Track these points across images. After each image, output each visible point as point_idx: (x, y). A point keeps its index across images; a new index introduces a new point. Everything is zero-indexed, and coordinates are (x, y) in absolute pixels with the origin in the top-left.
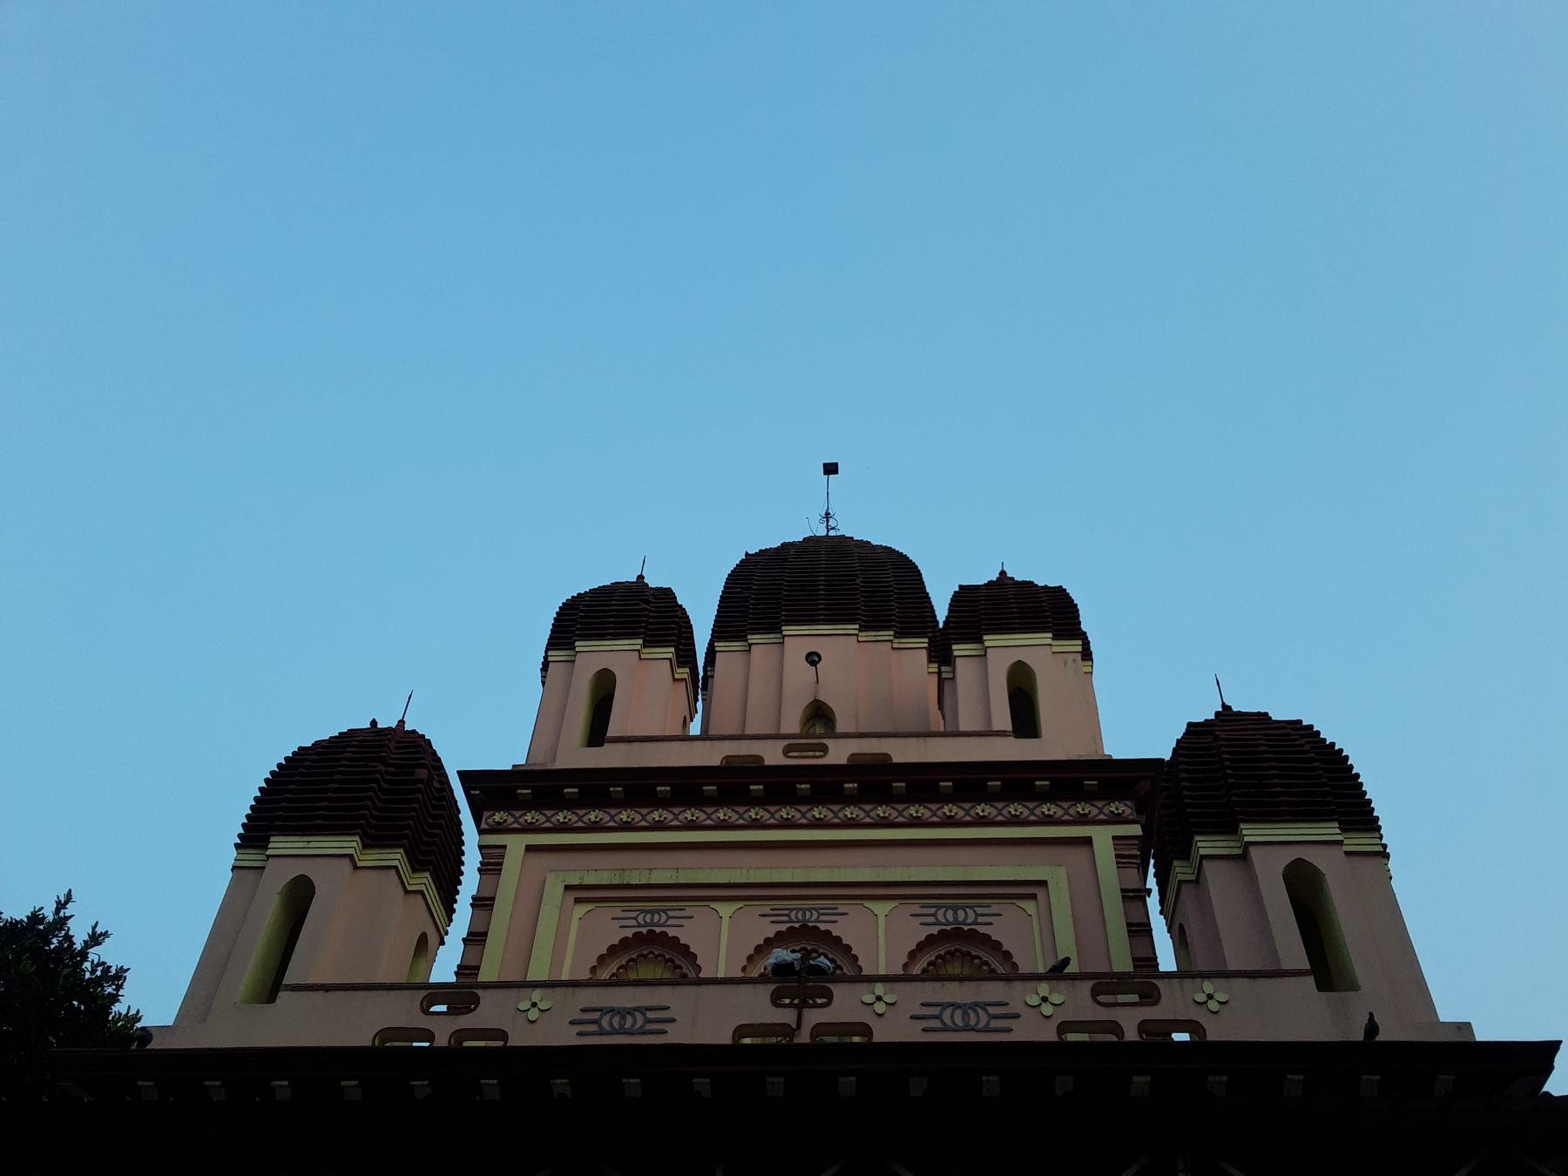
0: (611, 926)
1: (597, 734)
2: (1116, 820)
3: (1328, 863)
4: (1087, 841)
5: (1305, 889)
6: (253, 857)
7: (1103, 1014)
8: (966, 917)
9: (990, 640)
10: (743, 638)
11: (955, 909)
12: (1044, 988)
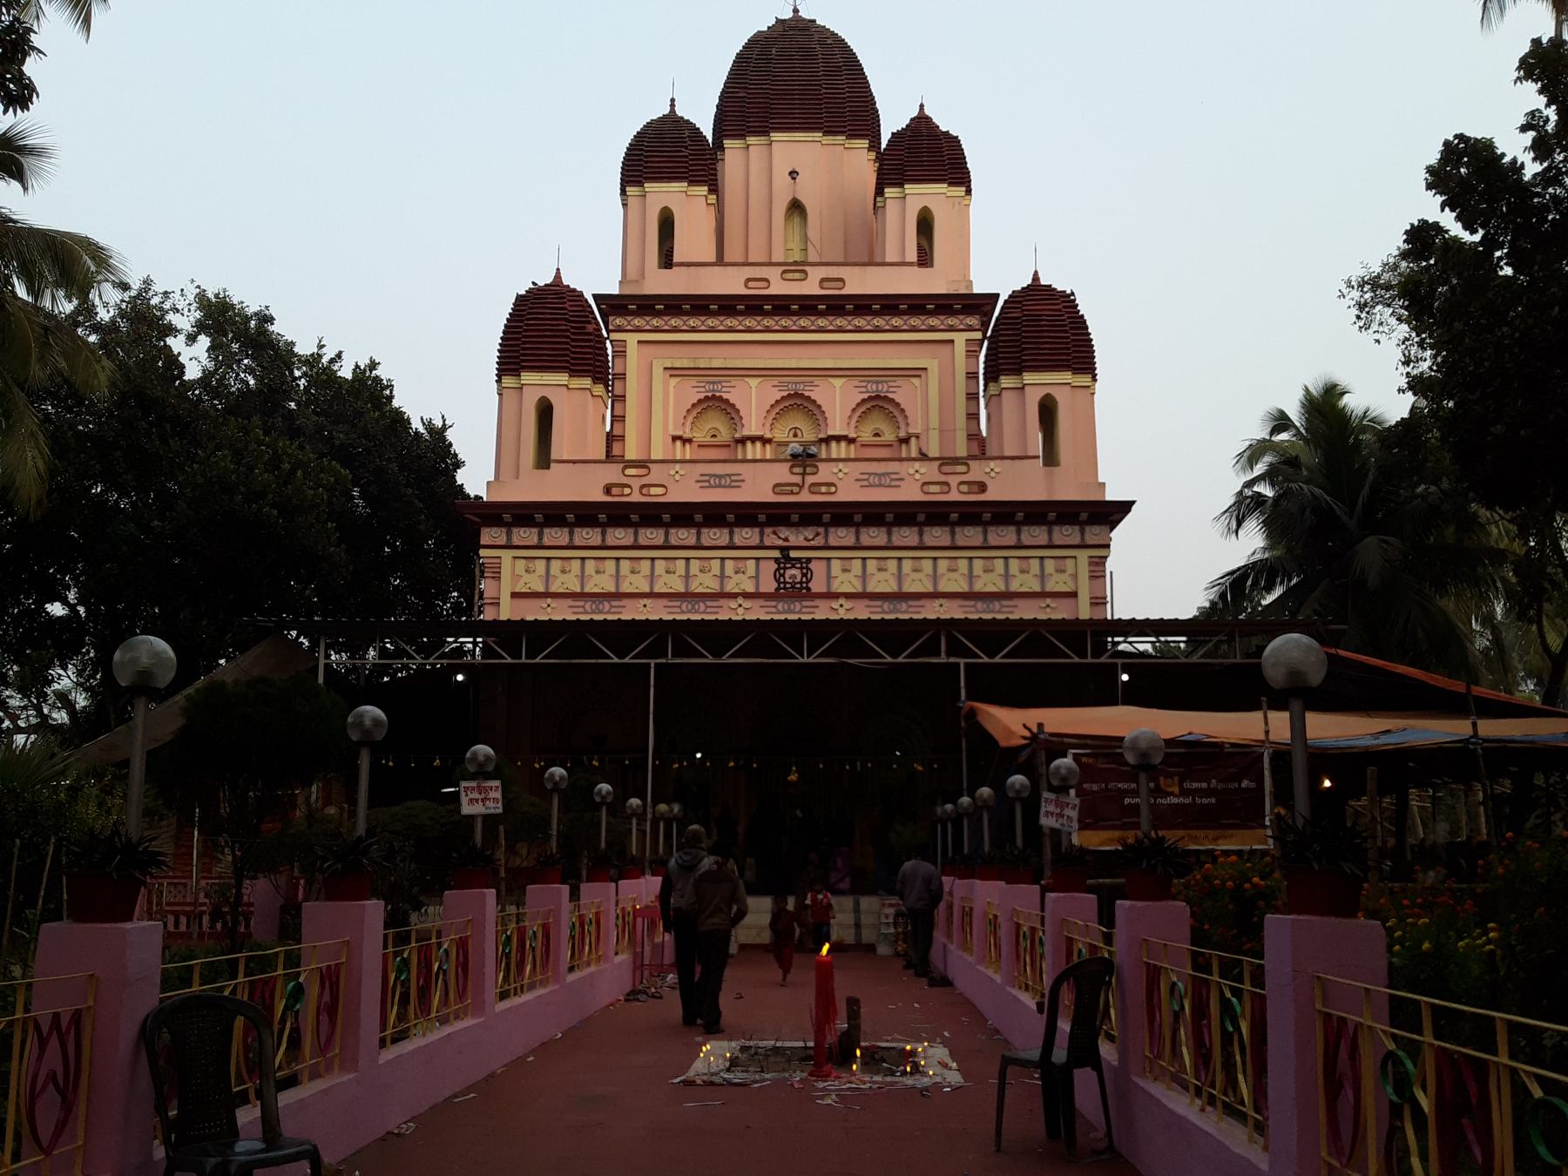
0: (693, 392)
1: (667, 260)
2: (970, 329)
3: (1061, 395)
5: (1047, 412)
6: (508, 381)
7: (943, 478)
8: (883, 389)
9: (910, 188)
12: (917, 465)
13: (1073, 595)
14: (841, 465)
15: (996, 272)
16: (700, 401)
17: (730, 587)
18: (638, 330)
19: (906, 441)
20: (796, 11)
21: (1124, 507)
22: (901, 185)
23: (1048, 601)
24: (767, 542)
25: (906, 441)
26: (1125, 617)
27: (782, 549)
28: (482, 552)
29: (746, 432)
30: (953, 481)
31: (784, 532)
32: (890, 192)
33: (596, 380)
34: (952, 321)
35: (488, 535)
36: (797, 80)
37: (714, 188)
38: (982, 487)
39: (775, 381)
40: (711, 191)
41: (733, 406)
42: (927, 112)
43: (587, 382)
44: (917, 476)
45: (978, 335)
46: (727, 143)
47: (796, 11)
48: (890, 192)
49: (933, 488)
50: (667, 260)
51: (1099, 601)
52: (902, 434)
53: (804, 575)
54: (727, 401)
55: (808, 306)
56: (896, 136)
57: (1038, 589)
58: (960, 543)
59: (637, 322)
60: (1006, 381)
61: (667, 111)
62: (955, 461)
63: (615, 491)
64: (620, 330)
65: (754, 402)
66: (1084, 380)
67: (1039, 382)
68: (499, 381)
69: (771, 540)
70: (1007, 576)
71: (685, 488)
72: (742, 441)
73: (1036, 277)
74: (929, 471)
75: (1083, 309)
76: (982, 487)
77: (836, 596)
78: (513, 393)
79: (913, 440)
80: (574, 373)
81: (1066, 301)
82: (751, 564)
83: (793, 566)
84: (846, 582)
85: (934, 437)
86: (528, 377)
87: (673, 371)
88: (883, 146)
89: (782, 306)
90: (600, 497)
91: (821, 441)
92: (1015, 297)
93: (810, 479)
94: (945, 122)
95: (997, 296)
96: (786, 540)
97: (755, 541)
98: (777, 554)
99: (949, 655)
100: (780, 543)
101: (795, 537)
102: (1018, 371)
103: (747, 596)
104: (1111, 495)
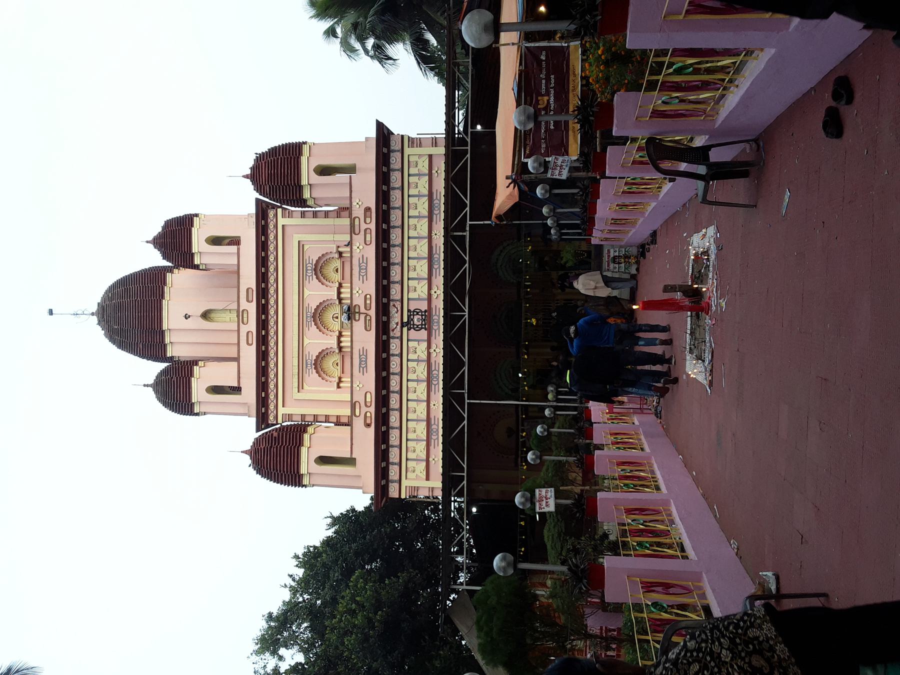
0: (312, 376)
1: (237, 390)
3: (314, 163)
4: (283, 226)
5: (324, 171)
6: (305, 481)
7: (362, 233)
8: (310, 267)
10: (165, 345)
11: (307, 270)
12: (355, 248)
13: (430, 156)
14: (354, 292)
15: (244, 199)
16: (317, 372)
17: (424, 356)
18: (276, 407)
19: (340, 254)
20: (93, 314)
21: (380, 126)
22: (193, 254)
23: (434, 172)
24: (399, 334)
25: (340, 254)
26: (444, 126)
27: (402, 327)
28: (403, 497)
29: (335, 346)
30: (364, 226)
31: (393, 325)
33: (305, 431)
34: (271, 226)
35: (393, 493)
36: (132, 314)
37: (195, 362)
38: (368, 209)
39: (306, 329)
40: (197, 364)
41: (320, 353)
42: (151, 238)
43: (306, 437)
44: (361, 247)
45: (280, 210)
46: (169, 355)
47: (93, 314)
49: (368, 238)
50: (237, 390)
51: (435, 142)
52: (337, 256)
53: (417, 314)
54: (317, 357)
55: (263, 309)
56: (165, 257)
57: (427, 178)
58: (400, 223)
59: (272, 407)
60: (306, 195)
61: (151, 389)
62: (352, 225)
63: (368, 421)
64: (276, 417)
65: (317, 341)
66: (305, 149)
67: (307, 175)
68: (306, 486)
70: (419, 196)
71: (368, 381)
72: (340, 348)
73: (246, 177)
74: (358, 240)
75: (265, 149)
76: (368, 209)
77: (430, 295)
79: (340, 249)
80: (300, 443)
81: (261, 159)
82: (411, 344)
83: (412, 320)
84: (422, 290)
85: (338, 237)
86: (303, 470)
87: (300, 387)
88: (170, 264)
89: (263, 324)
90: (372, 429)
91: (340, 303)
92: (259, 188)
93: (363, 310)
94: (157, 229)
95: (257, 200)
96: (397, 324)
97: (398, 341)
98: (405, 329)
99: (465, 231)
100: (399, 327)
101: (395, 319)
102: (300, 188)
103: (429, 347)
104: (373, 134)
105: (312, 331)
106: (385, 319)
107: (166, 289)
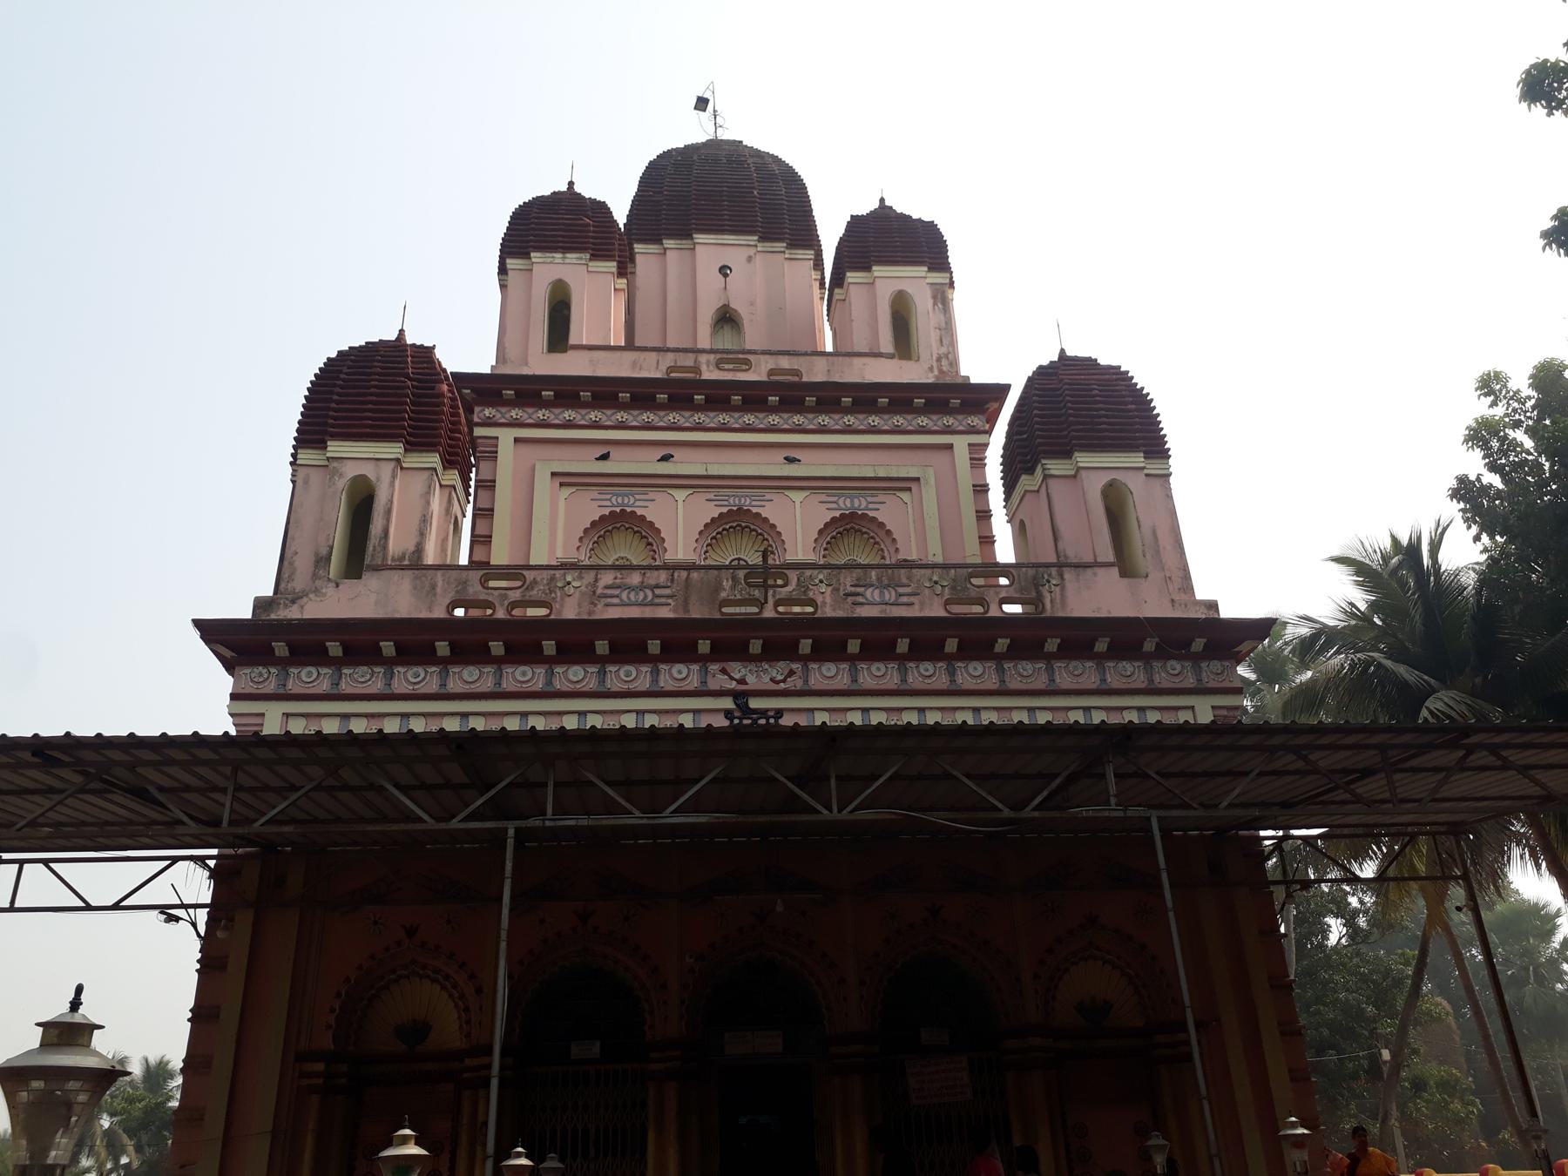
0: (592, 507)
3: (1135, 483)
4: (950, 447)
6: (306, 456)
8: (860, 504)
9: (878, 270)
10: (659, 241)
11: (852, 498)
22: (868, 269)
24: (713, 685)
27: (736, 695)
31: (738, 669)
32: (852, 277)
34: (949, 420)
41: (651, 524)
42: (887, 203)
48: (852, 277)
59: (515, 413)
60: (1056, 467)
66: (1154, 467)
67: (1098, 467)
69: (718, 681)
73: (1062, 351)
75: (1140, 380)
78: (316, 477)
80: (412, 446)
86: (336, 448)
89: (719, 397)
95: (1003, 390)
96: (742, 681)
97: (694, 683)
98: (728, 703)
102: (1068, 455)
105: (707, 509)
106: (756, 647)
107: (780, 246)
